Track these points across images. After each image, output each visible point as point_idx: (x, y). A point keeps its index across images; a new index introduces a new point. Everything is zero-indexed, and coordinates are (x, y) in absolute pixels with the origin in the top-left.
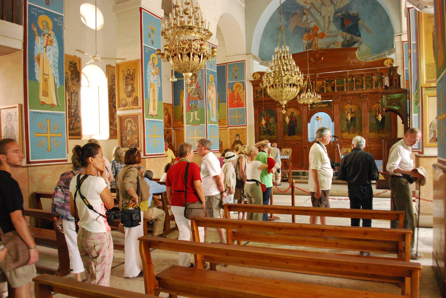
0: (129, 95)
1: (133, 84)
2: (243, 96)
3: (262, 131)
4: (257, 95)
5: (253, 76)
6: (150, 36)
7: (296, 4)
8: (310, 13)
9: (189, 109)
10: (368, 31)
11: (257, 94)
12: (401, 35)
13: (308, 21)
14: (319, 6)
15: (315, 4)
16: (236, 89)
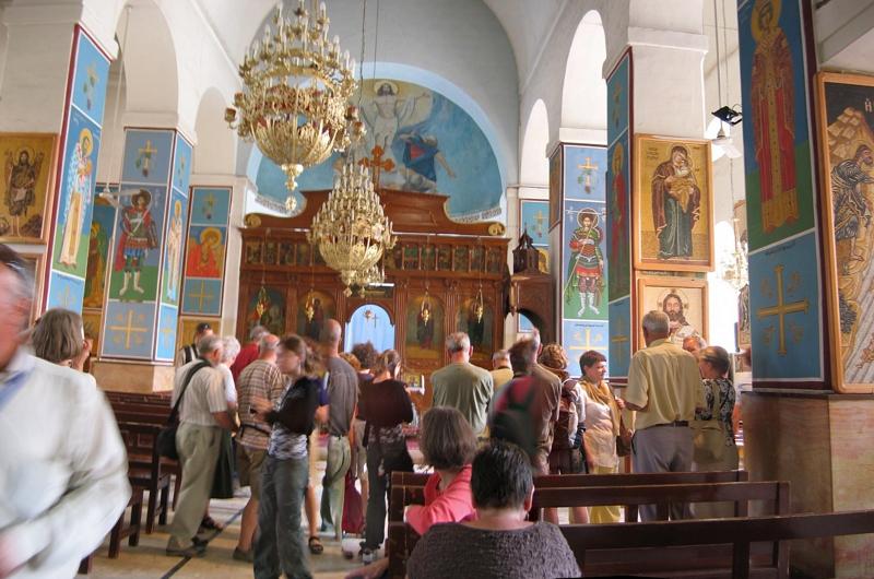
0: (15, 209)
1: (32, 186)
2: (222, 255)
6: (85, 89)
9: (121, 265)
10: (449, 173)
11: (249, 255)
12: (518, 188)
15: (367, 109)
16: (206, 240)
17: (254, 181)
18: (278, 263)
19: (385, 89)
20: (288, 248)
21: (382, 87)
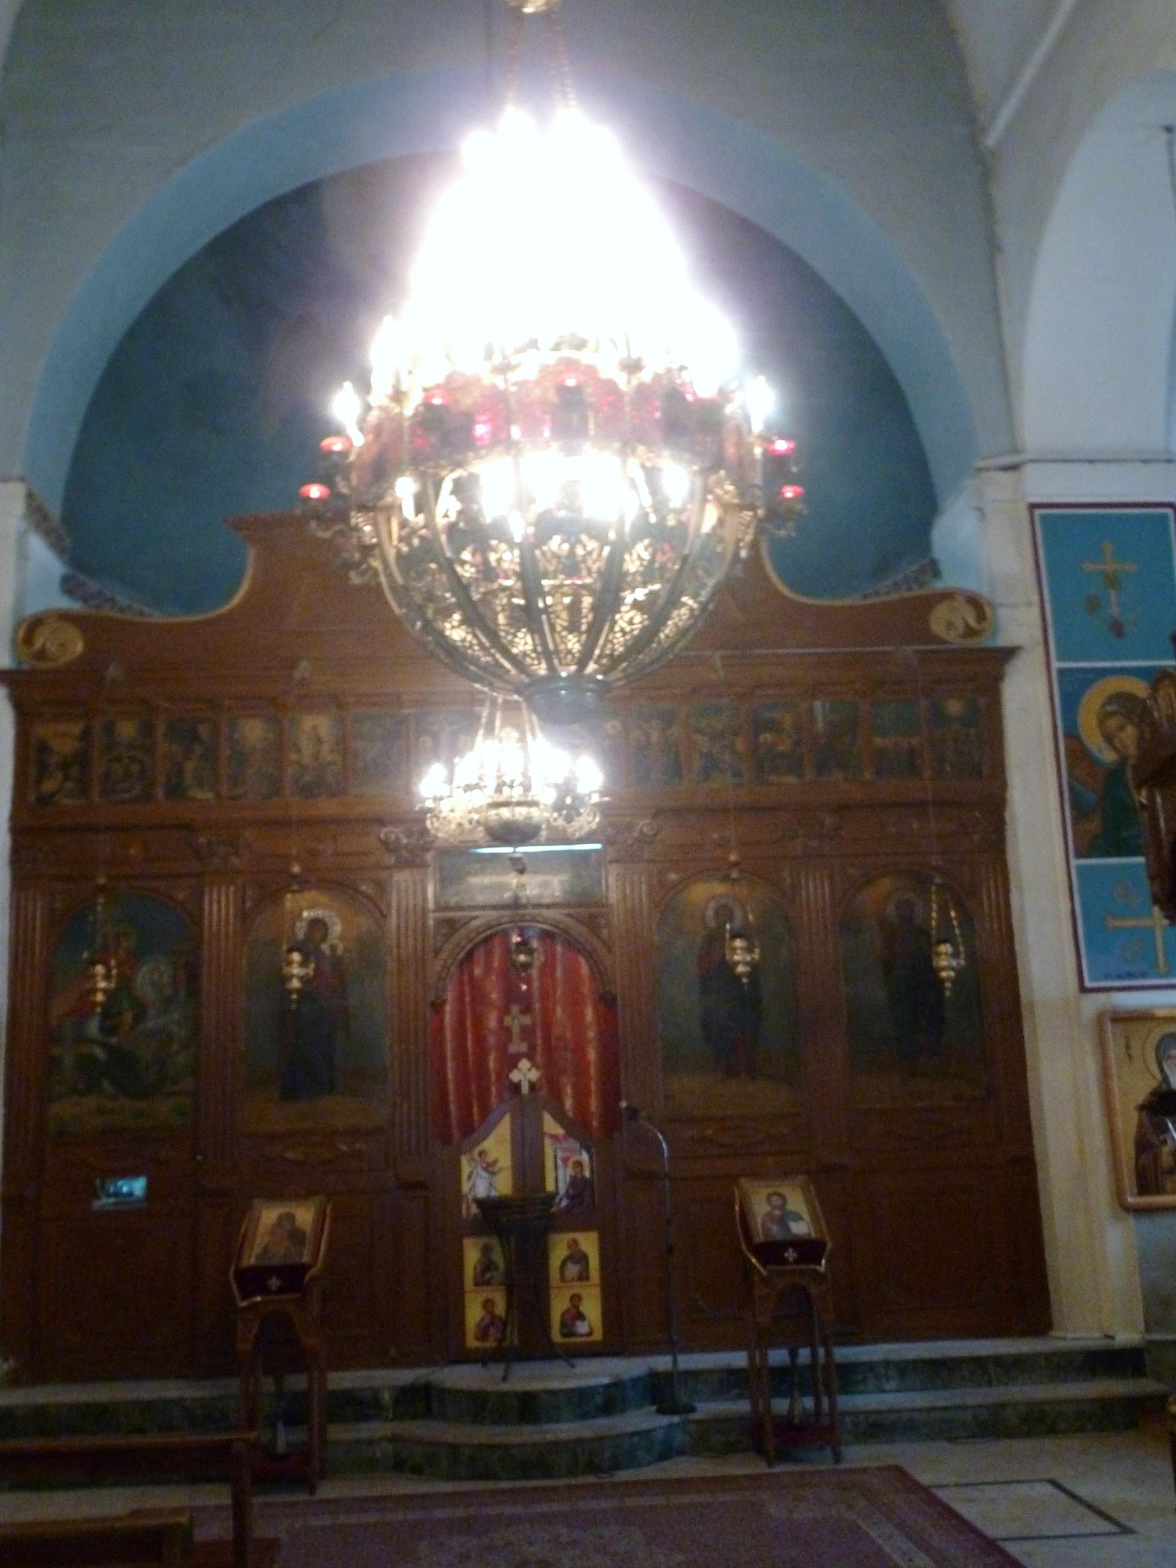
3: (68, 1061)
4: (49, 786)
5: (28, 639)
17: (55, 510)
18: (160, 793)
20: (196, 738)
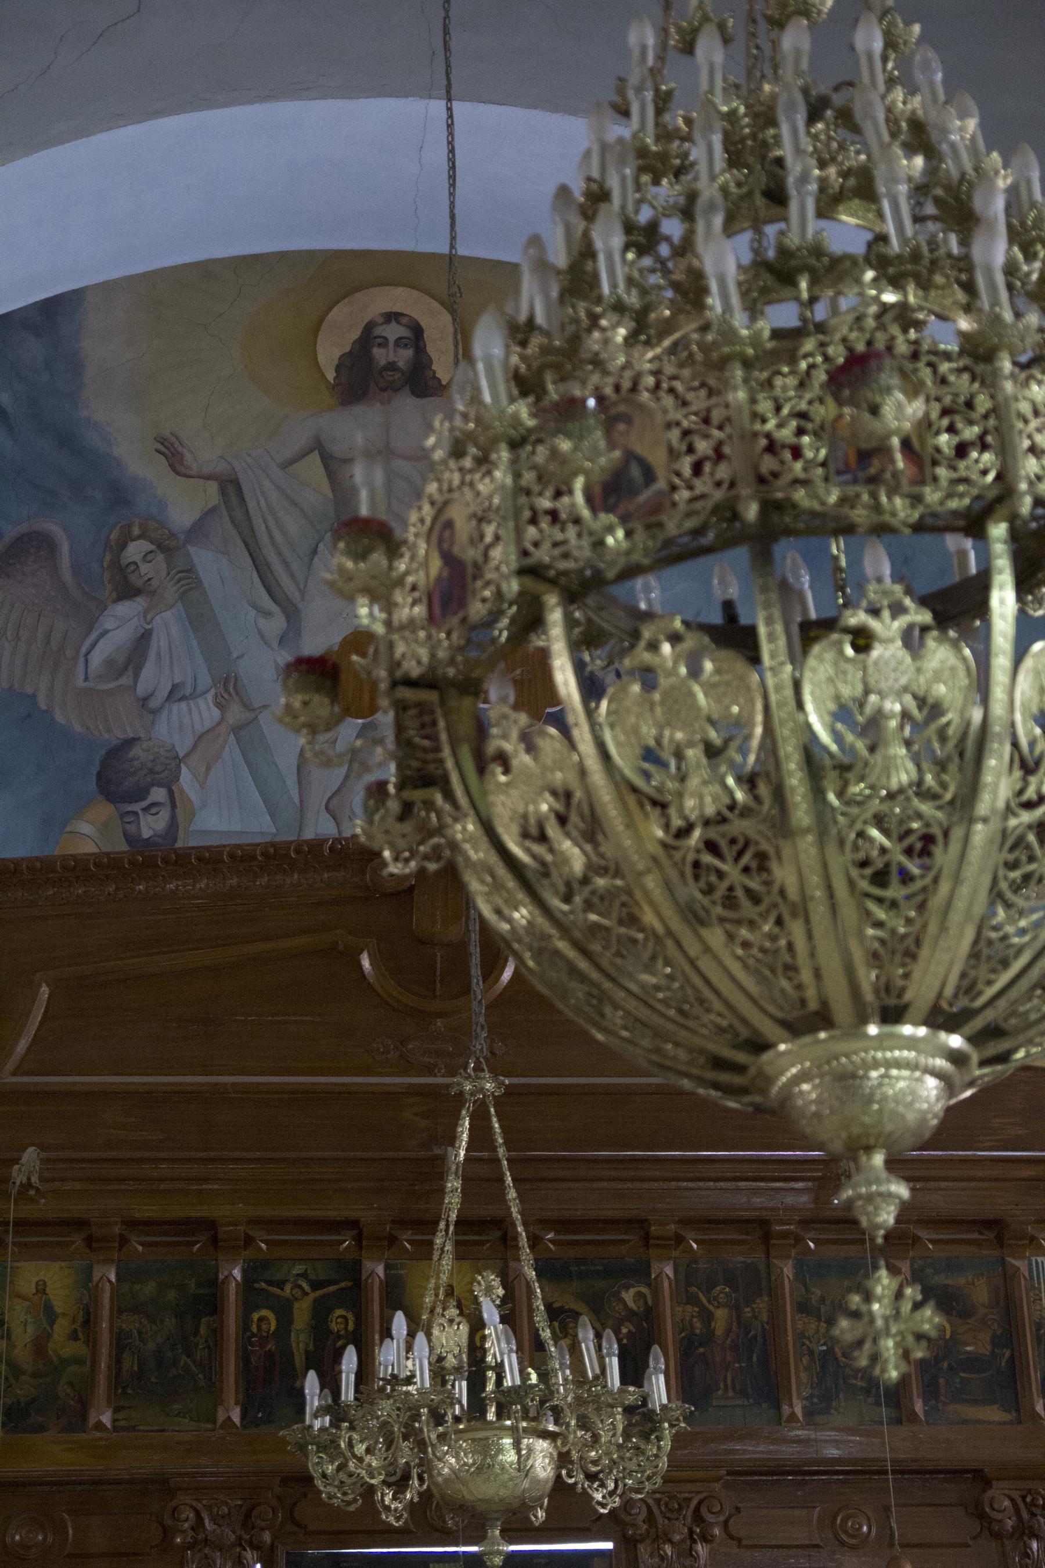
7: (68, 440)
8: (189, 579)
13: (152, 678)
14: (293, 525)
19: (381, 356)
21: (368, 338)
